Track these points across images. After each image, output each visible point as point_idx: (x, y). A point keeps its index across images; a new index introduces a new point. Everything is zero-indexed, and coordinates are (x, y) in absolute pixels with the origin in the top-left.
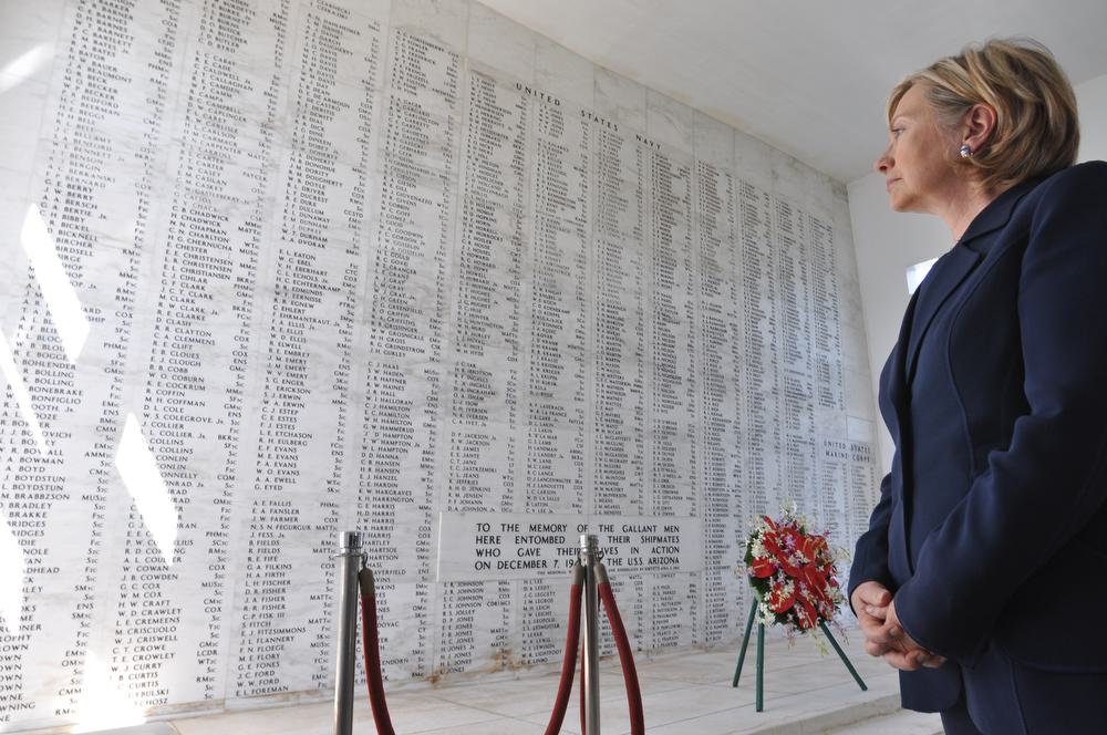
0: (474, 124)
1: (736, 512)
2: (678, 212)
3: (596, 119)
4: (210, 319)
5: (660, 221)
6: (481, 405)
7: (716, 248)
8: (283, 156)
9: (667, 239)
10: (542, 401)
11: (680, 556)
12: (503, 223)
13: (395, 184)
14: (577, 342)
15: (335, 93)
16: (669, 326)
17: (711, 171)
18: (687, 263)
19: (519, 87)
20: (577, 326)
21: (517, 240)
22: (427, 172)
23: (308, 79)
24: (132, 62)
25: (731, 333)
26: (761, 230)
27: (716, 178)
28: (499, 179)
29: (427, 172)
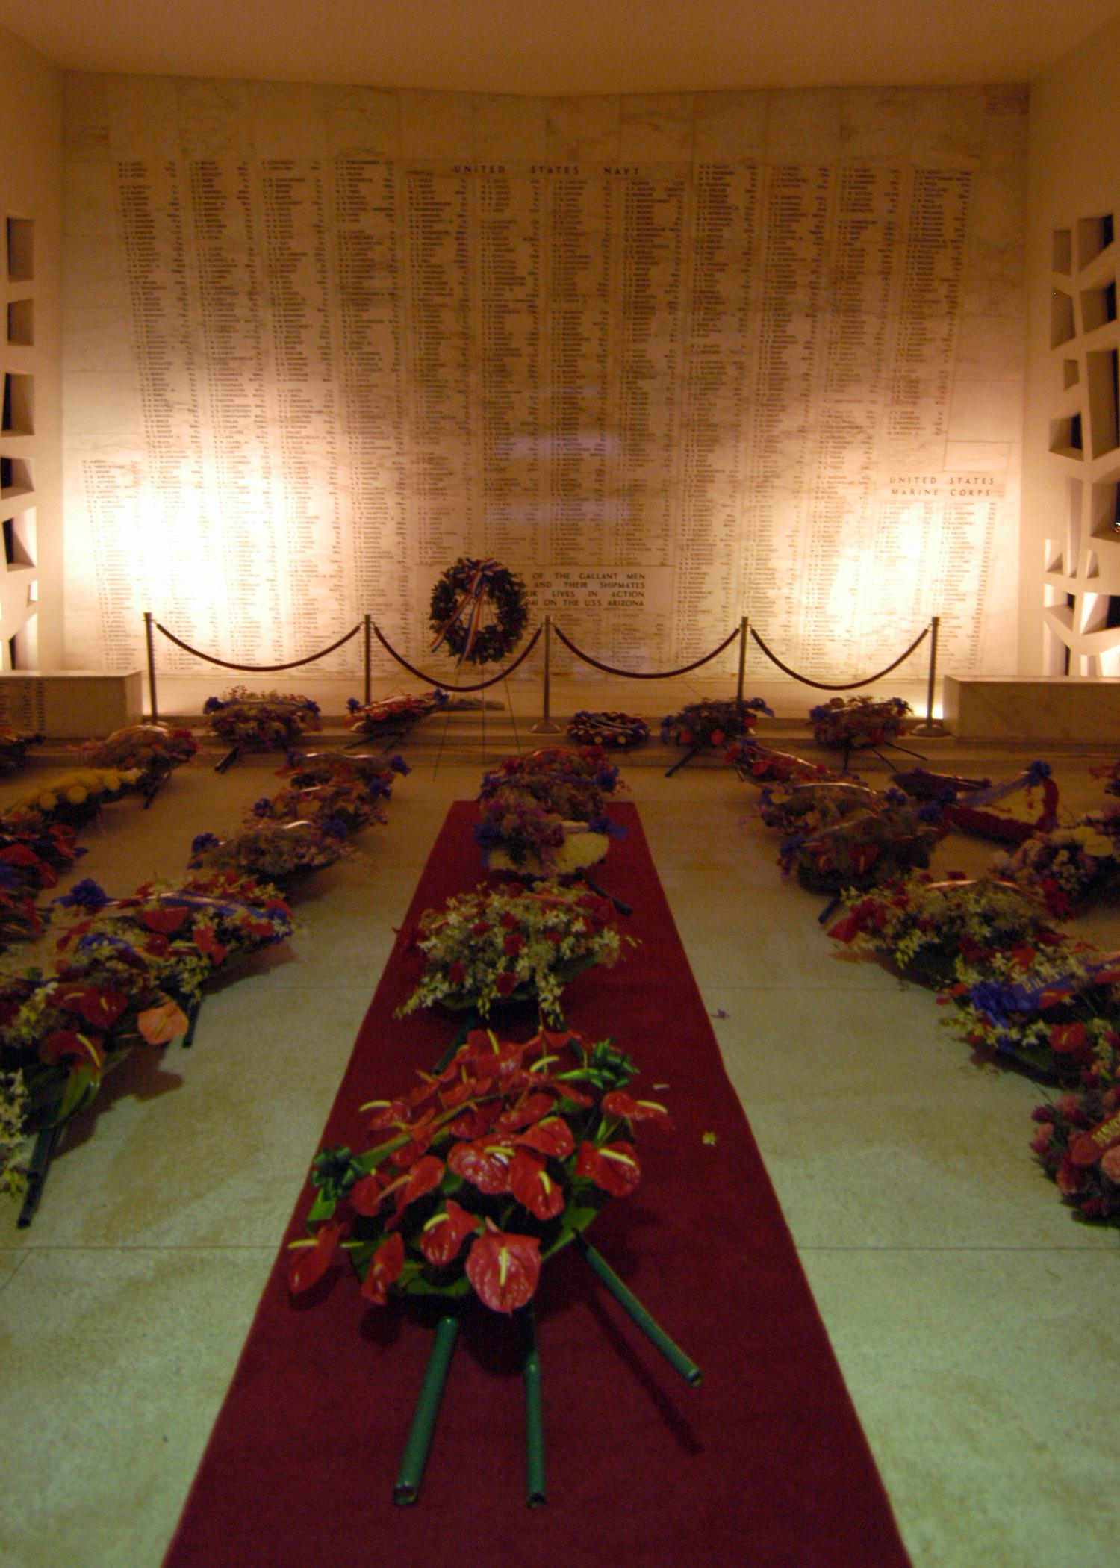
0: (415, 230)
1: (724, 560)
2: (662, 246)
3: (550, 171)
4: (245, 446)
5: (634, 266)
6: (441, 484)
7: (718, 275)
8: (266, 314)
9: (643, 283)
10: (496, 475)
11: (644, 600)
12: (449, 321)
13: (352, 312)
14: (530, 419)
15: (295, 245)
16: (640, 383)
17: (721, 171)
18: (672, 306)
19: (456, 170)
20: (529, 403)
21: (465, 335)
22: (376, 294)
23: (273, 240)
24: (161, 275)
25: (732, 371)
26: (803, 227)
27: (728, 179)
28: (444, 279)
29: (376, 294)
